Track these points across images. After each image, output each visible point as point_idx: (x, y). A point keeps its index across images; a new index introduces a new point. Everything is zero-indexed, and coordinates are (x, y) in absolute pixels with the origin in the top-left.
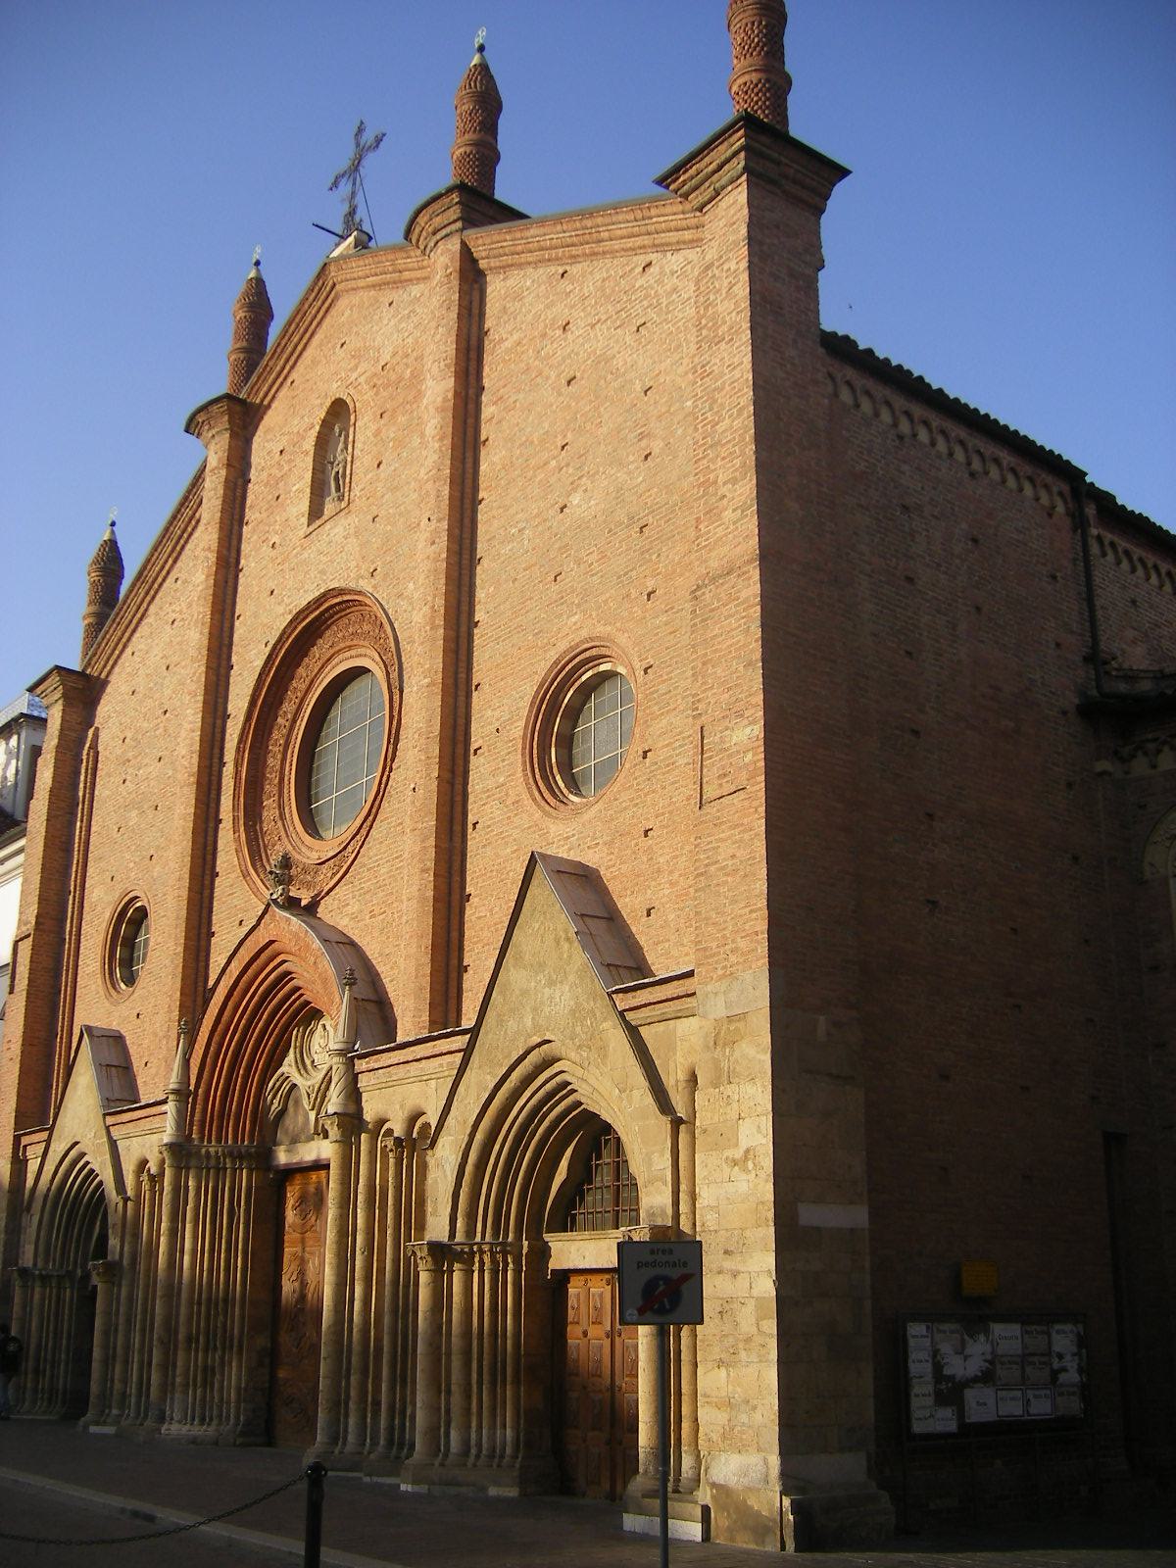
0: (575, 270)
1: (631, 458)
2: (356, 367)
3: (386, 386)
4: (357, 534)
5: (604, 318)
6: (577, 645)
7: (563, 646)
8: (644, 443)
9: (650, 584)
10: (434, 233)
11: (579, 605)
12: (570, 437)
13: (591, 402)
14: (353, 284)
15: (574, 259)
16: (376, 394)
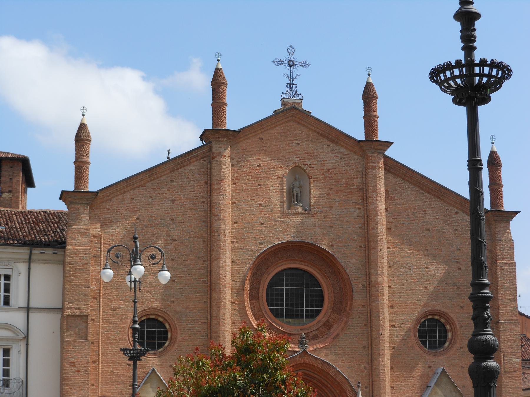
0: (428, 195)
1: (453, 266)
2: (310, 160)
3: (331, 178)
4: (319, 227)
5: (441, 218)
6: (434, 310)
7: (429, 309)
8: (458, 264)
9: (462, 305)
10: (376, 149)
11: (434, 299)
12: (428, 248)
13: (437, 242)
14: (307, 125)
15: (428, 192)
16: (325, 178)
